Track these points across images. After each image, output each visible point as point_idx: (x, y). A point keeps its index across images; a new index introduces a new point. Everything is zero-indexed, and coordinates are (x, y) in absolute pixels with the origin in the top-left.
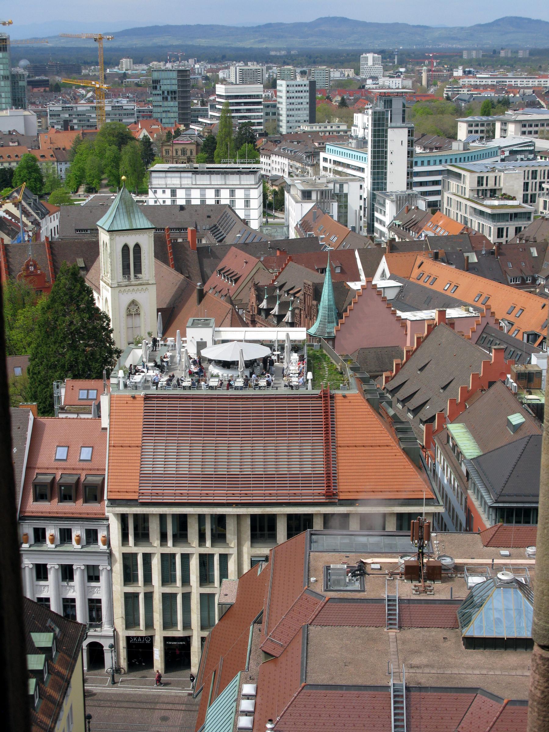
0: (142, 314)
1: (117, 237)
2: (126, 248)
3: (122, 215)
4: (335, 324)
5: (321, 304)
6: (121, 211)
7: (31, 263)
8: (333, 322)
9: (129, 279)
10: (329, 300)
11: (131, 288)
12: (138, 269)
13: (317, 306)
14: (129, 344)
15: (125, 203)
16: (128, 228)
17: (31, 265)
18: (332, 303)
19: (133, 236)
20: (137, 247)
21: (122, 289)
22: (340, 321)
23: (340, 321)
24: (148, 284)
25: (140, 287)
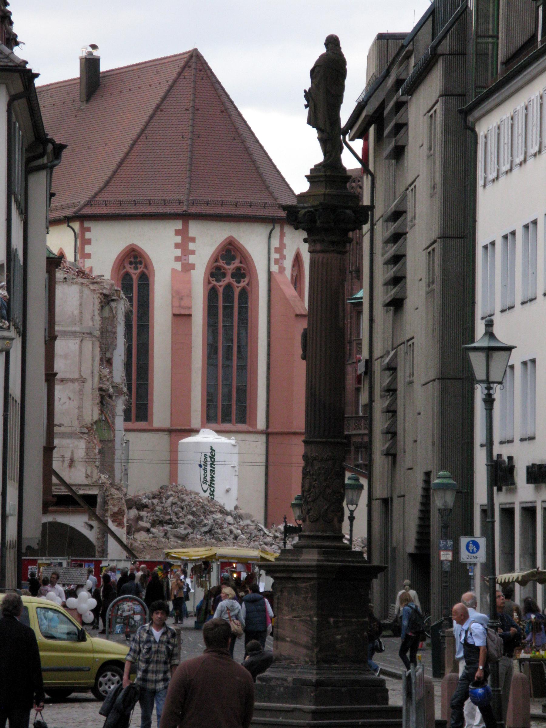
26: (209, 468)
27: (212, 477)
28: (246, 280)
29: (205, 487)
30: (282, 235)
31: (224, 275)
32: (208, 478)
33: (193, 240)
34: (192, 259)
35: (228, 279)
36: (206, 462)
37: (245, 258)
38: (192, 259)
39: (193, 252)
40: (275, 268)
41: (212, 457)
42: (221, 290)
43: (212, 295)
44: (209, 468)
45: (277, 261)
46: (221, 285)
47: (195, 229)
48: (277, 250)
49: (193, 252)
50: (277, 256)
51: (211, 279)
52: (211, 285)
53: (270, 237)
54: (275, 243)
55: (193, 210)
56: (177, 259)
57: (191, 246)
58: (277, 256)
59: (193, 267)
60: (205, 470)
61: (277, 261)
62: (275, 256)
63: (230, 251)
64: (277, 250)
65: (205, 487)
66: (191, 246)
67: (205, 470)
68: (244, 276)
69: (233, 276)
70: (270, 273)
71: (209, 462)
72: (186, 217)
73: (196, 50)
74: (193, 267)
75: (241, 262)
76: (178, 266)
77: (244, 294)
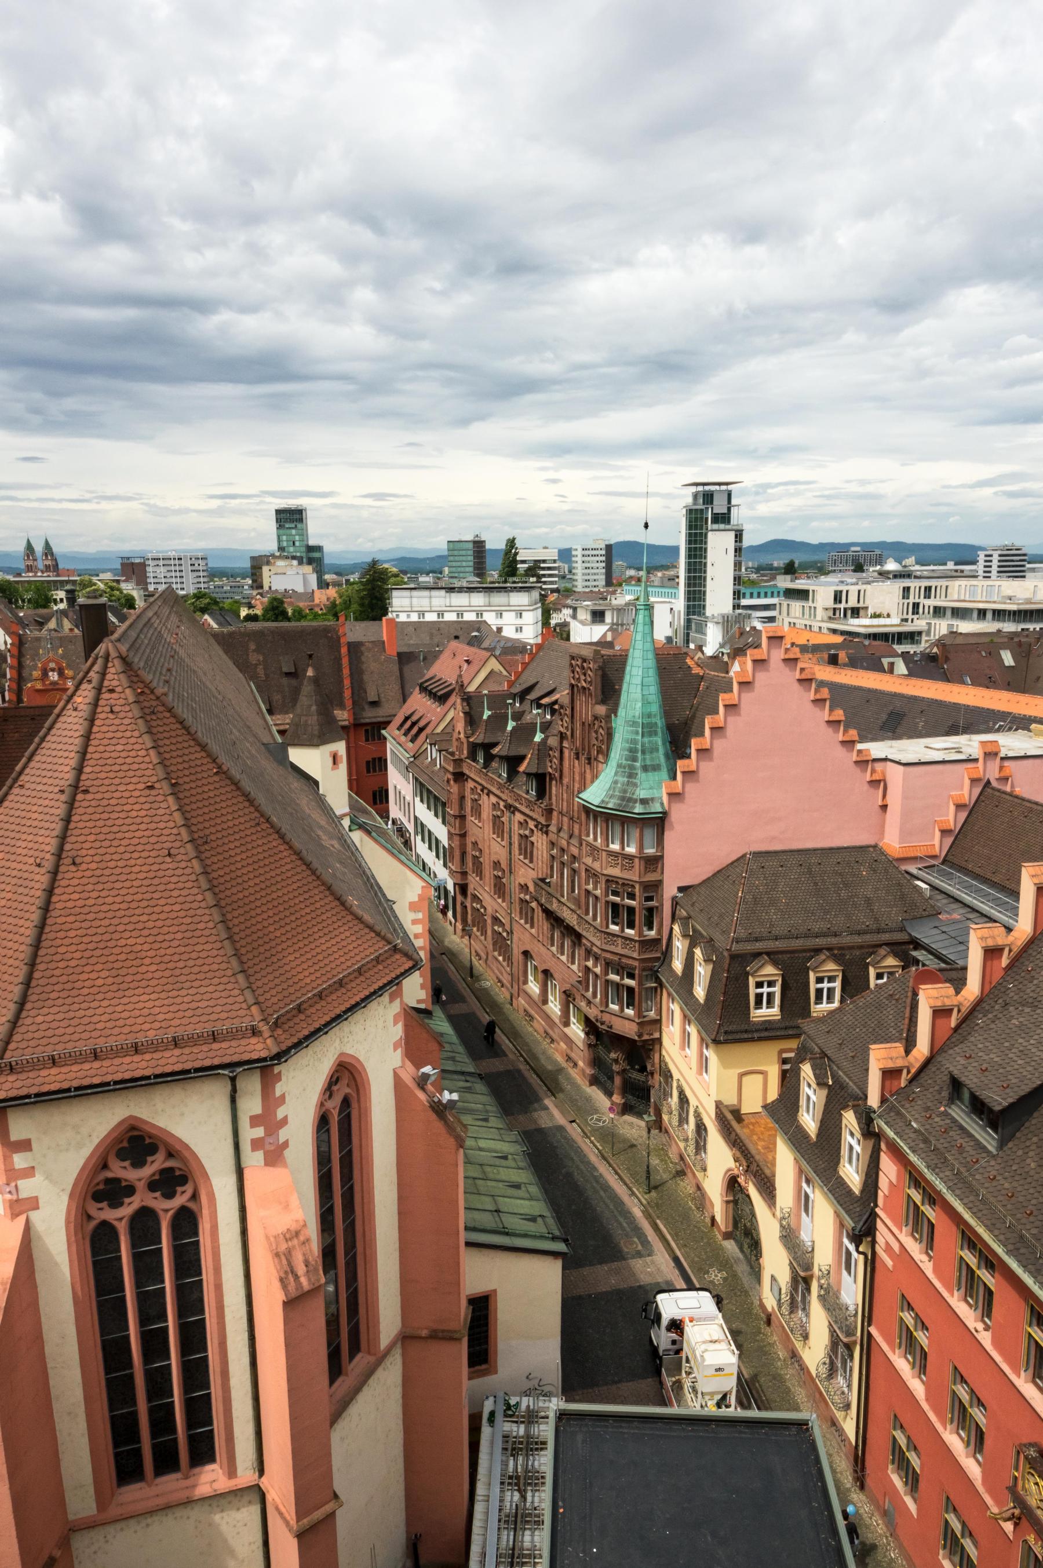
4: (664, 774)
5: (621, 712)
7: (52, 665)
8: (656, 768)
10: (645, 702)
13: (608, 718)
17: (53, 670)
18: (655, 708)
22: (679, 763)
23: (681, 765)
28: (189, 1189)
34: (27, 1187)
38: (27, 1187)
42: (122, 1229)
43: (97, 1244)
46: (119, 1216)
48: (255, 1121)
50: (259, 1132)
51: (93, 1208)
52: (93, 1224)
53: (233, 1100)
59: (33, 1204)
61: (256, 1144)
62: (249, 1133)
63: (136, 1143)
68: (183, 1180)
69: (152, 1186)
74: (33, 1204)
75: (170, 1155)
77: (187, 1222)
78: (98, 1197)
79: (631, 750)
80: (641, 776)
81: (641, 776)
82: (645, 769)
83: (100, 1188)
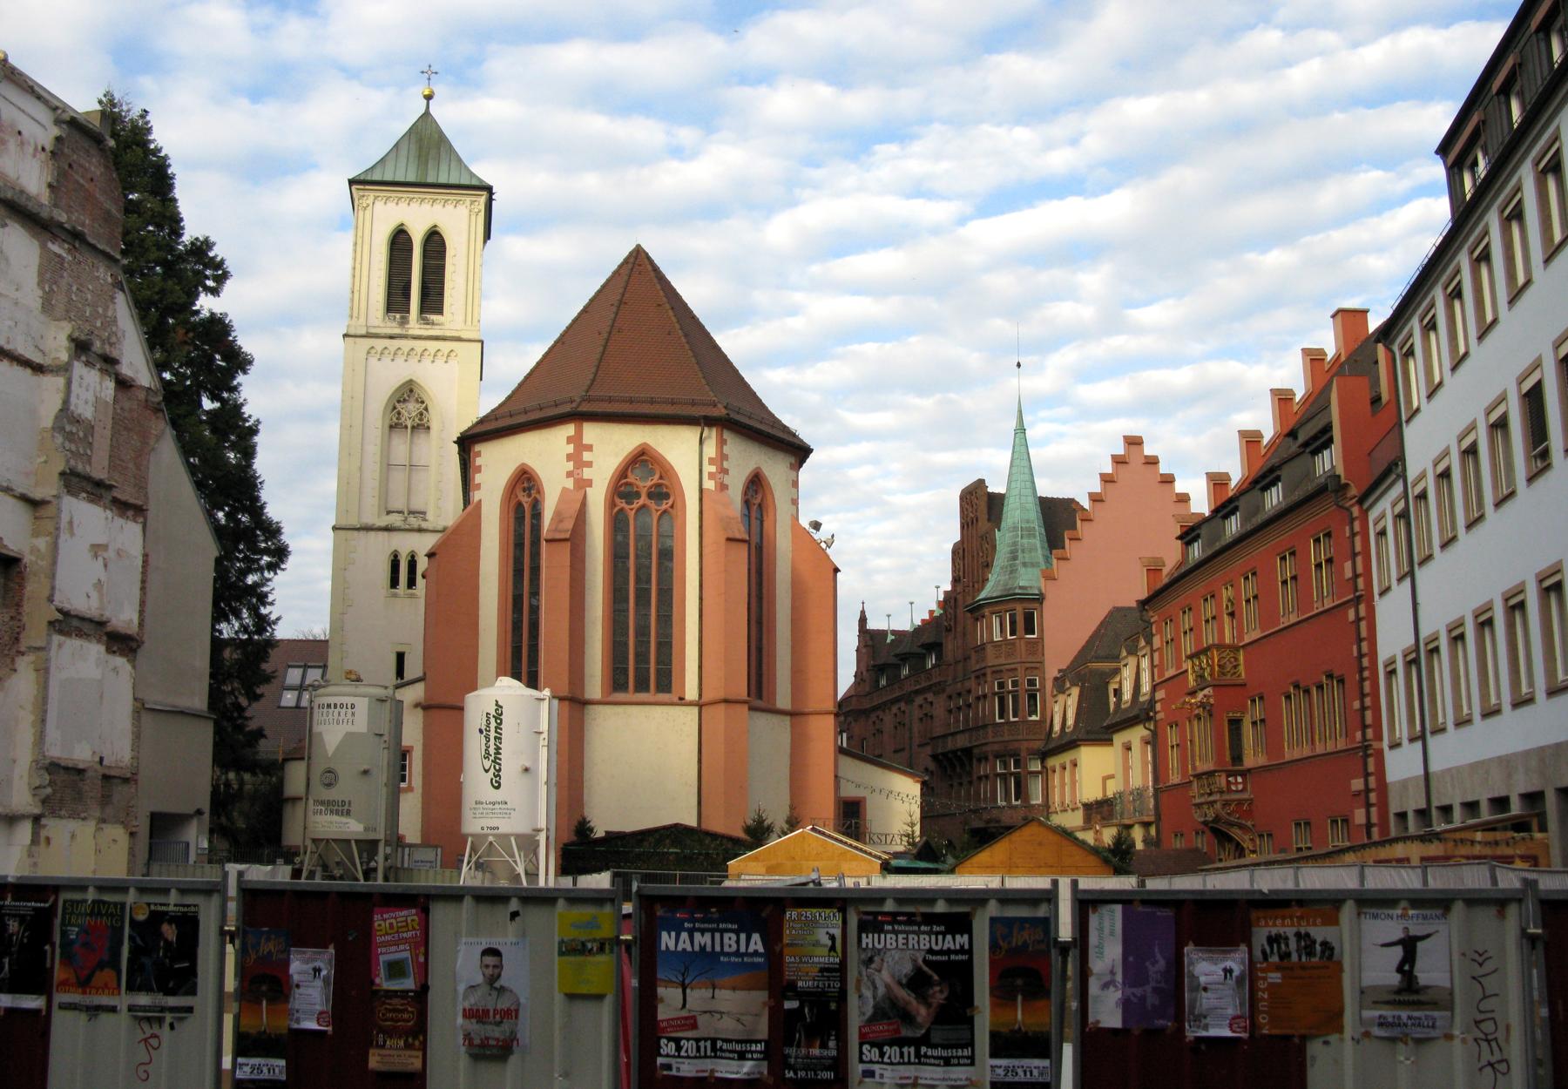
0: (434, 425)
1: (379, 205)
2: (400, 240)
3: (403, 160)
6: (403, 152)
9: (404, 322)
11: (406, 344)
12: (433, 300)
14: (388, 513)
15: (420, 140)
16: (411, 178)
19: (426, 206)
20: (435, 243)
21: (380, 344)
24: (459, 339)
25: (433, 346)
26: (492, 734)
27: (498, 749)
29: (487, 764)
30: (721, 442)
31: (638, 495)
32: (492, 751)
33: (589, 448)
34: (587, 473)
35: (643, 500)
36: (488, 725)
37: (666, 471)
38: (587, 473)
39: (589, 464)
40: (709, 485)
41: (498, 717)
44: (492, 734)
45: (711, 476)
47: (593, 432)
48: (711, 461)
49: (589, 464)
50: (713, 469)
51: (618, 501)
54: (710, 450)
55: (585, 408)
56: (569, 474)
57: (586, 456)
58: (713, 469)
59: (589, 483)
60: (487, 738)
61: (711, 476)
64: (711, 461)
65: (487, 764)
66: (586, 456)
67: (487, 738)
68: (667, 496)
69: (650, 496)
70: (701, 490)
71: (493, 724)
72: (579, 417)
73: (638, 246)
74: (589, 483)
76: (570, 484)
78: (623, 496)
79: (1012, 552)
80: (1022, 570)
81: (1022, 570)
82: (1025, 564)
83: (621, 489)
